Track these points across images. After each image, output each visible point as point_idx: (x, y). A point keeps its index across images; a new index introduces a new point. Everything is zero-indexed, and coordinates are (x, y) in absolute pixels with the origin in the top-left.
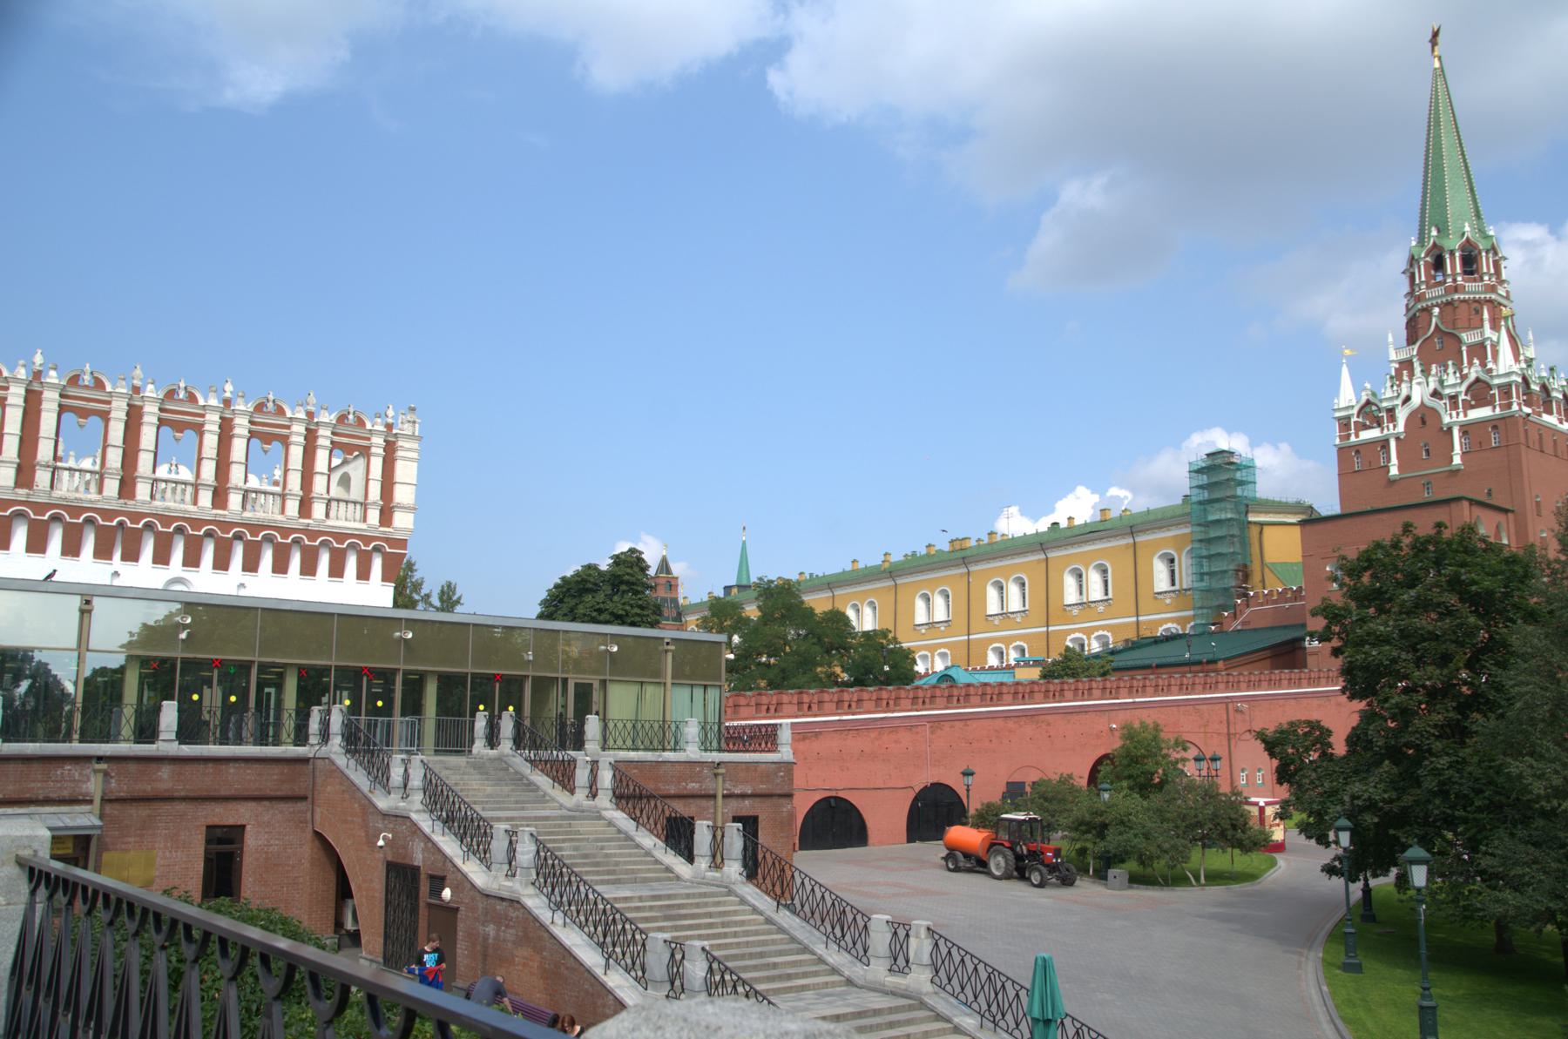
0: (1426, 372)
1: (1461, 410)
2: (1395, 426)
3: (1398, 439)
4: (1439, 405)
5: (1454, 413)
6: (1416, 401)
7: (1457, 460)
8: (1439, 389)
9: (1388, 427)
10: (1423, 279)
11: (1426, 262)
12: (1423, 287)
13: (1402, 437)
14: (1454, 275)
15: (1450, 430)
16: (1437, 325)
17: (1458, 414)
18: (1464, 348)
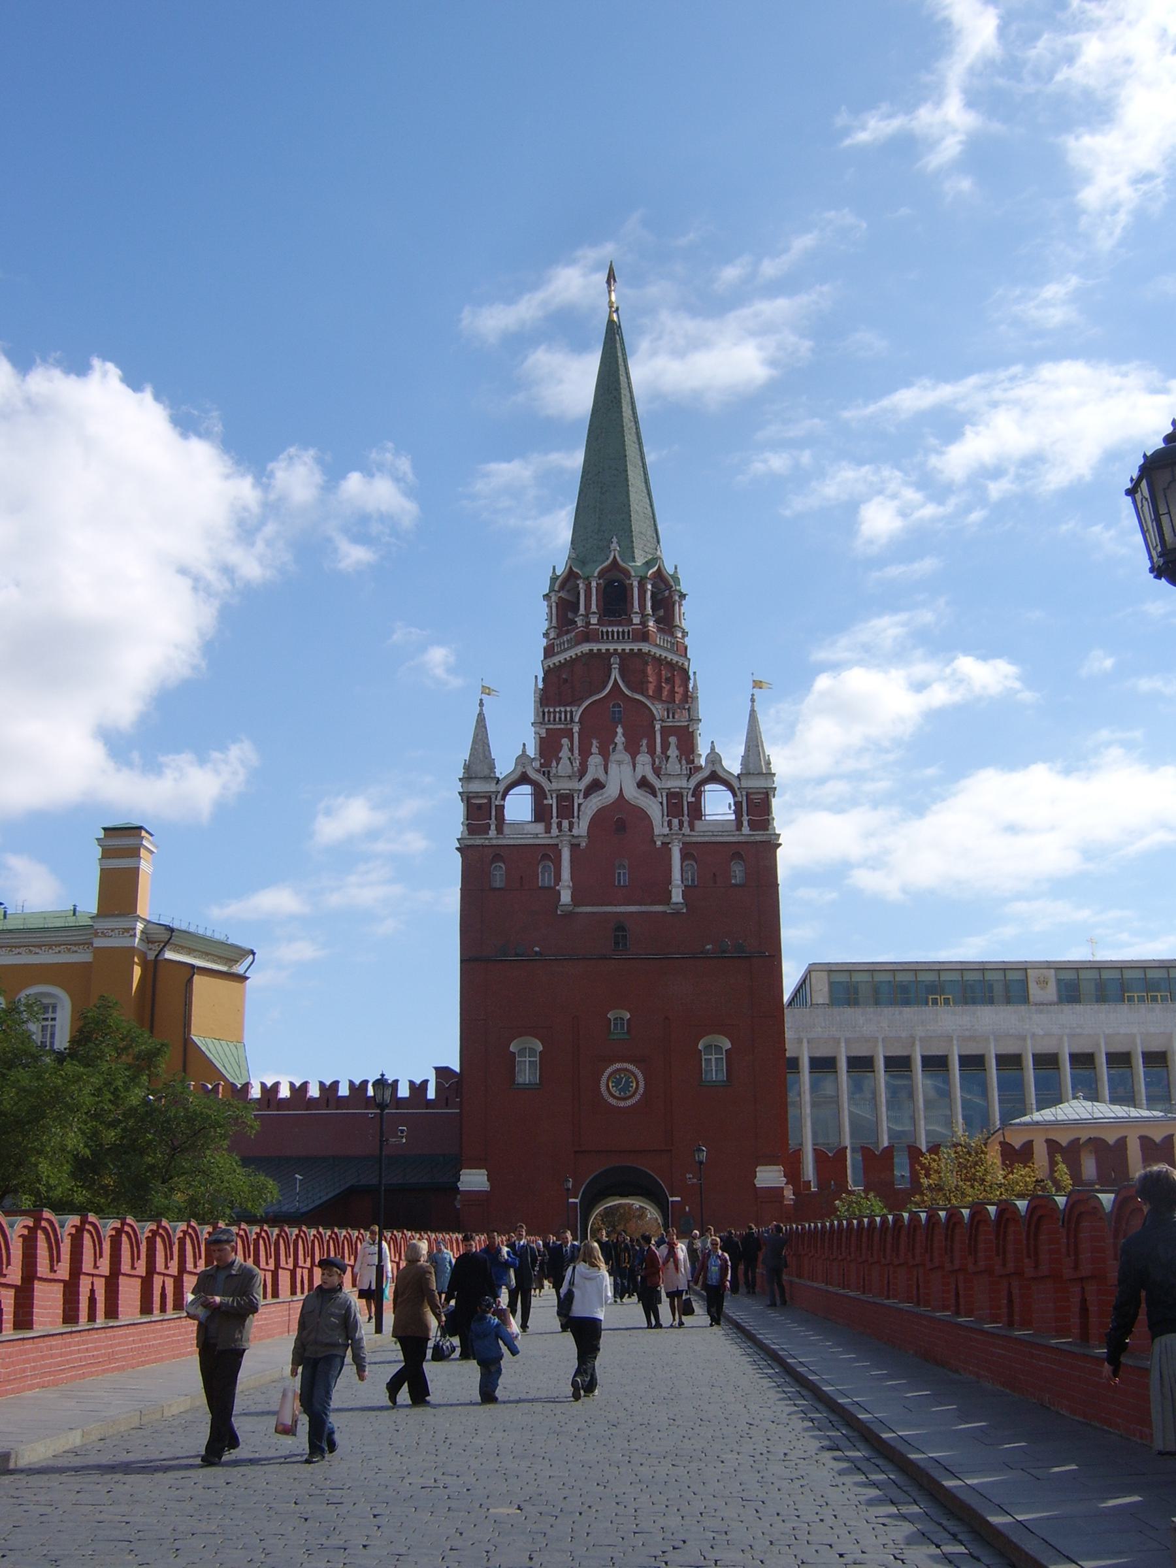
0: (633, 750)
1: (686, 818)
2: (571, 825)
3: (574, 847)
4: (654, 809)
7: (677, 896)
8: (652, 778)
9: (559, 825)
10: (594, 608)
12: (594, 620)
14: (644, 616)
16: (615, 679)
17: (681, 824)
18: (658, 727)
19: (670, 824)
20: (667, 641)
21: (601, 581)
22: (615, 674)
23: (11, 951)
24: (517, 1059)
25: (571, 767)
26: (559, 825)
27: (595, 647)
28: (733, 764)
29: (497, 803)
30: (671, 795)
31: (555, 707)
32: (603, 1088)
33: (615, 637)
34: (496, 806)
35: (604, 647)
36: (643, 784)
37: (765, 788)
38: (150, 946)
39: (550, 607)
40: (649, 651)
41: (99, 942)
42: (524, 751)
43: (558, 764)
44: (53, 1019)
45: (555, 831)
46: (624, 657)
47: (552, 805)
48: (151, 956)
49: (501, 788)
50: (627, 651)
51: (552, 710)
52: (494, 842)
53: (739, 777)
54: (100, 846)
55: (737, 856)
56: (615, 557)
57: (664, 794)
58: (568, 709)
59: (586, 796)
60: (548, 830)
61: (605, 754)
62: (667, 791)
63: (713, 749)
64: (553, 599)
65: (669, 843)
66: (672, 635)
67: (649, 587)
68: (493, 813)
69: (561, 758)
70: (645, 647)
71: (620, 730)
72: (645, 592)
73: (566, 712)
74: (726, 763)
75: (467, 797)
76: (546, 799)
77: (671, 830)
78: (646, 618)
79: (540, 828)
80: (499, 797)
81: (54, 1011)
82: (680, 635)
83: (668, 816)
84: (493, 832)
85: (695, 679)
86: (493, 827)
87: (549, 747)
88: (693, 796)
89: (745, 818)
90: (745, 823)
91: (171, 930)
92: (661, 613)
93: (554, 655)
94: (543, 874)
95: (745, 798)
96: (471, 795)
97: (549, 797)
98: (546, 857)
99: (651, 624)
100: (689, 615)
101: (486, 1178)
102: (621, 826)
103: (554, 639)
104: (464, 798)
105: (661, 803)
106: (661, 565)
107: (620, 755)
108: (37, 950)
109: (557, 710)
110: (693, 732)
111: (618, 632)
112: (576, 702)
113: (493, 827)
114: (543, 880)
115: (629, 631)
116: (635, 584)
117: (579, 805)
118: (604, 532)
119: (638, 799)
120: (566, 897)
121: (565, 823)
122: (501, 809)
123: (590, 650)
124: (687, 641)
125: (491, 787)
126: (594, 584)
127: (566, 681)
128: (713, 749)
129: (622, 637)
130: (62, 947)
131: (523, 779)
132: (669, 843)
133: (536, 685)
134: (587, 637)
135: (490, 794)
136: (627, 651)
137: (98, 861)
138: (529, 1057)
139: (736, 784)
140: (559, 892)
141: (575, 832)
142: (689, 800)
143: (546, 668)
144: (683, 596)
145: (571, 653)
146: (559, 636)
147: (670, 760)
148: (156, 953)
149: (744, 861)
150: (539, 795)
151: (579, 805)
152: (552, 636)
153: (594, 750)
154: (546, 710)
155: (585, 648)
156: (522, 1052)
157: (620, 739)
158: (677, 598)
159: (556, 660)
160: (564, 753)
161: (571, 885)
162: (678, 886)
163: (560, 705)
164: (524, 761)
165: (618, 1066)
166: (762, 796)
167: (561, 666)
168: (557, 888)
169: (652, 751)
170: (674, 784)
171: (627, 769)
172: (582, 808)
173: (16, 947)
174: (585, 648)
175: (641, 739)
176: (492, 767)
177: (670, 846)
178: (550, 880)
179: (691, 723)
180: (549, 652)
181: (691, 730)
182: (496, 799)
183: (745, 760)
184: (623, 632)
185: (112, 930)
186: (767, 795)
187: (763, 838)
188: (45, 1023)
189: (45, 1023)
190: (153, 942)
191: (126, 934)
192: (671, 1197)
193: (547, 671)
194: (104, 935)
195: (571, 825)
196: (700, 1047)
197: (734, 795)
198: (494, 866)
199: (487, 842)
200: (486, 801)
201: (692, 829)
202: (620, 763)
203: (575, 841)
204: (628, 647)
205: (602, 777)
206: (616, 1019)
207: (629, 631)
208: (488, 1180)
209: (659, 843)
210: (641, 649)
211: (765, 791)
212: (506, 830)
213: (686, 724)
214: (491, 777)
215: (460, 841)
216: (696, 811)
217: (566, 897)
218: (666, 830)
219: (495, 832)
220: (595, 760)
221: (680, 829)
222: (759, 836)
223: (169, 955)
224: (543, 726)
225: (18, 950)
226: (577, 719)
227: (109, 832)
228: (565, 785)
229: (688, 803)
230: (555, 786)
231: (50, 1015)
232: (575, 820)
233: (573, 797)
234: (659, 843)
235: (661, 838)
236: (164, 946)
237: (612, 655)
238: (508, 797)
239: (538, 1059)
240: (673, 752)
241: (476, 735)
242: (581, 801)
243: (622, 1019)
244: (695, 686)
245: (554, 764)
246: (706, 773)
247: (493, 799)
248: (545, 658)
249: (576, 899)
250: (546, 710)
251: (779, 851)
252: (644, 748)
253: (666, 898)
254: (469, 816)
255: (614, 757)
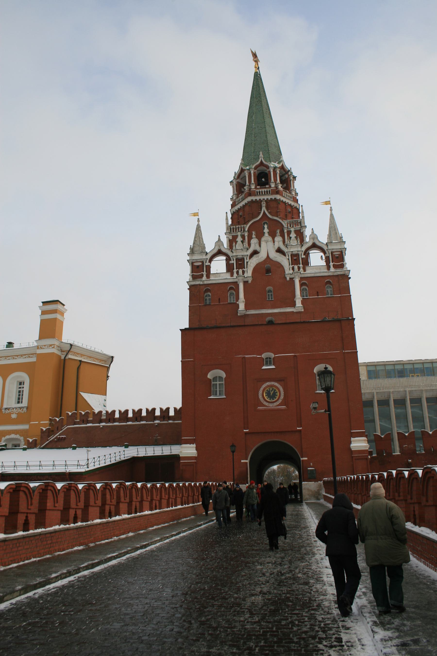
1: (301, 265)
2: (243, 272)
3: (245, 283)
4: (285, 261)
5: (296, 267)
6: (262, 256)
7: (299, 303)
8: (283, 248)
9: (238, 273)
10: (253, 181)
11: (254, 172)
12: (253, 187)
13: (250, 281)
15: (292, 279)
16: (264, 212)
17: (299, 268)
18: (285, 231)
19: (293, 269)
20: (288, 196)
21: (256, 171)
22: (264, 209)
23: (6, 358)
24: (212, 383)
25: (242, 245)
26: (238, 273)
27: (254, 198)
28: (323, 239)
29: (207, 264)
30: (293, 255)
31: (236, 225)
32: (260, 397)
33: (263, 193)
34: (206, 266)
35: (258, 198)
36: (279, 251)
37: (340, 249)
38: (63, 353)
39: (233, 187)
40: (280, 199)
41: (39, 351)
42: (219, 239)
43: (236, 244)
44: (23, 388)
45: (235, 275)
46: (267, 201)
47: (233, 264)
48: (63, 357)
49: (209, 257)
50: (269, 199)
51: (234, 227)
52: (206, 283)
53: (327, 244)
54: (41, 310)
55: (329, 282)
56: (261, 160)
57: (290, 255)
58: (242, 226)
59: (250, 258)
60: (232, 275)
61: (260, 236)
62: (291, 253)
63: (313, 232)
64: (235, 182)
65: (294, 278)
66: (290, 193)
67: (278, 172)
68: (205, 269)
69: (237, 241)
70: (278, 197)
71: (266, 226)
72: (276, 174)
73: (241, 228)
74: (320, 239)
75: (192, 263)
76: (231, 260)
77: (294, 271)
78: (277, 185)
79: (228, 276)
80: (208, 261)
81: (24, 384)
82: (294, 193)
83: (292, 265)
84: (204, 278)
85: (302, 209)
86: (205, 276)
87: (232, 242)
88: (304, 255)
89: (331, 264)
90: (332, 267)
91: (71, 345)
92: (285, 185)
93: (236, 205)
94: (230, 297)
95: (330, 254)
96: (193, 261)
97: (232, 259)
98: (231, 288)
99: (280, 187)
100: (298, 185)
101: (195, 449)
102: (268, 271)
103: (235, 199)
104: (191, 263)
105: (289, 259)
106: (284, 164)
107: (267, 237)
108: (16, 357)
109: (237, 227)
110: (303, 232)
111: (265, 192)
112: (246, 223)
113: (205, 276)
114: (230, 301)
115: (270, 191)
116: (272, 170)
117: (247, 262)
118: (256, 152)
119: (276, 258)
120: (242, 306)
121: (240, 271)
122: (209, 268)
123: (252, 200)
124: (297, 198)
125: (204, 257)
126: (252, 172)
127: (241, 216)
128: (313, 232)
129: (267, 193)
130: (26, 355)
131: (219, 253)
132: (294, 278)
133: (227, 219)
134: (250, 194)
135: (203, 260)
136: (269, 199)
137: (39, 316)
138: (219, 381)
139: (325, 248)
140: (238, 305)
141: (246, 275)
142: (302, 257)
143: (232, 213)
144: (295, 178)
145: (243, 203)
146: (237, 198)
147: (292, 239)
148: (64, 356)
149: (332, 285)
150: (228, 259)
151: (247, 262)
152: (234, 198)
153: (254, 236)
154: (232, 227)
155: (249, 199)
156: (215, 379)
157: (266, 230)
158: (292, 178)
159: (236, 208)
160: (239, 239)
161: (244, 300)
162: (299, 299)
163: (239, 224)
164: (219, 244)
165: (268, 383)
166: (339, 253)
167: (239, 210)
168: (237, 303)
169: (282, 235)
170: (295, 250)
171: (271, 244)
172: (249, 263)
173: (8, 357)
174: (249, 199)
175: (277, 229)
176: (203, 247)
177: (294, 279)
178: (233, 301)
179: (301, 228)
180: (233, 206)
181: (301, 232)
182: (206, 262)
183: (330, 236)
184: (267, 191)
185: (45, 346)
186: (342, 252)
187: (342, 273)
188: (20, 389)
189: (20, 389)
190: (64, 351)
191: (50, 347)
192: (302, 457)
193: (233, 214)
194: (41, 348)
195: (243, 272)
196: (315, 371)
197: (325, 253)
198: (206, 294)
199: (201, 283)
200: (200, 264)
201: (305, 270)
202: (267, 242)
203: (246, 280)
204: (269, 197)
205: (257, 248)
206: (267, 358)
207: (270, 191)
208: (197, 450)
209: (288, 279)
210: (276, 198)
211: (340, 250)
212: (212, 278)
213: (299, 229)
214: (203, 252)
215: (189, 283)
216: (306, 262)
217: (242, 306)
218: (291, 271)
219: (206, 278)
220: (254, 241)
221: (299, 270)
222: (339, 272)
223: (70, 356)
224: (230, 234)
225: (9, 358)
226: (246, 230)
227: (44, 304)
228: (240, 254)
229: (302, 258)
230: (234, 254)
231: (22, 386)
232: (245, 270)
233: (244, 259)
234: (288, 279)
235: (289, 275)
236: (68, 353)
237: (262, 201)
238: (212, 262)
239: (224, 382)
240: (293, 235)
241: (196, 234)
242: (247, 261)
243: (270, 358)
244: (303, 217)
245: (234, 244)
246: (310, 244)
247: (205, 263)
248: (232, 207)
249: (247, 307)
250: (232, 227)
251: (349, 280)
252: (278, 234)
253: (293, 304)
254: (192, 271)
255: (263, 239)
